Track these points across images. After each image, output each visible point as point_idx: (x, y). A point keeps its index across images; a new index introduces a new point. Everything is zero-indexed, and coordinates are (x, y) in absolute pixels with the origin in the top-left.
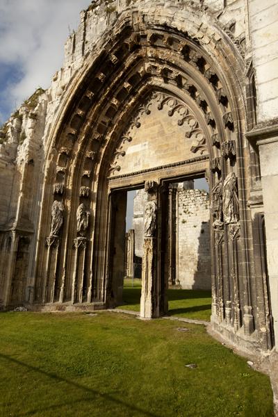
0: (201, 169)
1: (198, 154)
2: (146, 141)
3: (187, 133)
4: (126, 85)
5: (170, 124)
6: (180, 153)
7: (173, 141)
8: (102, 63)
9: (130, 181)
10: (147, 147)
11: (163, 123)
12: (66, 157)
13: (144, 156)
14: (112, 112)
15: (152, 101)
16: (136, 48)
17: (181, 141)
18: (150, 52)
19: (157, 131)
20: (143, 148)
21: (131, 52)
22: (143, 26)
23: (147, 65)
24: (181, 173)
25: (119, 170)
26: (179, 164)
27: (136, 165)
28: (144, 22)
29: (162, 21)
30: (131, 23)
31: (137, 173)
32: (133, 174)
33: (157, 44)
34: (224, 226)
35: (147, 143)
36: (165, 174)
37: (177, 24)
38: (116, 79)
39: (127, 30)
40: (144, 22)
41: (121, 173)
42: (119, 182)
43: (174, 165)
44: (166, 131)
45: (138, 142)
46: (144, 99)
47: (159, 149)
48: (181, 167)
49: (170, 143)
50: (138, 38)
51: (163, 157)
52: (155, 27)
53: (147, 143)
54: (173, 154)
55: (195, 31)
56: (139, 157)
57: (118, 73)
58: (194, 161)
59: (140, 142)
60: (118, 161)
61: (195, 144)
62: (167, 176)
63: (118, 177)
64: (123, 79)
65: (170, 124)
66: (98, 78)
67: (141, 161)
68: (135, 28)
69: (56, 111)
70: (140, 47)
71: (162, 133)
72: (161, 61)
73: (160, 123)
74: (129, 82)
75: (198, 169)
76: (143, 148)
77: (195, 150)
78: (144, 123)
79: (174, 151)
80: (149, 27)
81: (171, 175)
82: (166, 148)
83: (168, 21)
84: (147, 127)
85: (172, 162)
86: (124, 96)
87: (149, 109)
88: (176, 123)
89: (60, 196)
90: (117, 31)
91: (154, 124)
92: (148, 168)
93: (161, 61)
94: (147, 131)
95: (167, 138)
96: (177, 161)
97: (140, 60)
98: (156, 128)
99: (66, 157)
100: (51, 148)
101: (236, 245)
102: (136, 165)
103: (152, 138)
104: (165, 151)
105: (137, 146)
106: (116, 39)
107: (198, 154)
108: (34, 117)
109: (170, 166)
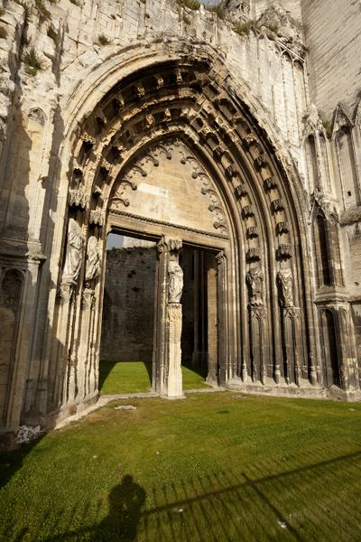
0: (220, 246)
1: (218, 231)
2: (165, 188)
3: (211, 206)
5: (193, 185)
7: (196, 205)
10: (167, 196)
12: (87, 147)
13: (164, 205)
14: (142, 129)
15: (172, 146)
16: (197, 88)
18: (206, 106)
19: (178, 184)
20: (162, 194)
21: (190, 87)
22: (221, 82)
23: (192, 113)
24: (202, 242)
25: (127, 206)
31: (157, 222)
33: (221, 107)
35: (167, 192)
36: (188, 236)
38: (166, 99)
39: (204, 66)
40: (225, 80)
41: (129, 210)
45: (153, 183)
46: (169, 139)
47: (181, 206)
48: (205, 237)
49: (193, 205)
50: (207, 83)
52: (234, 97)
54: (195, 220)
56: (157, 202)
57: (169, 94)
60: (124, 192)
61: (215, 220)
62: (190, 240)
63: (120, 213)
64: (168, 103)
66: (157, 81)
67: (159, 209)
68: (211, 73)
69: (95, 68)
70: (200, 91)
71: (185, 191)
72: (214, 125)
74: (171, 111)
77: (215, 226)
78: (163, 166)
79: (196, 216)
80: (228, 90)
81: (193, 241)
83: (251, 107)
84: (168, 173)
87: (187, 162)
88: (199, 189)
91: (175, 175)
92: (167, 221)
93: (214, 125)
94: (169, 178)
95: (190, 199)
96: (199, 229)
97: (191, 102)
98: (178, 181)
100: (75, 123)
102: (152, 210)
103: (173, 189)
105: (154, 187)
106: (191, 62)
107: (218, 231)
108: (51, 33)
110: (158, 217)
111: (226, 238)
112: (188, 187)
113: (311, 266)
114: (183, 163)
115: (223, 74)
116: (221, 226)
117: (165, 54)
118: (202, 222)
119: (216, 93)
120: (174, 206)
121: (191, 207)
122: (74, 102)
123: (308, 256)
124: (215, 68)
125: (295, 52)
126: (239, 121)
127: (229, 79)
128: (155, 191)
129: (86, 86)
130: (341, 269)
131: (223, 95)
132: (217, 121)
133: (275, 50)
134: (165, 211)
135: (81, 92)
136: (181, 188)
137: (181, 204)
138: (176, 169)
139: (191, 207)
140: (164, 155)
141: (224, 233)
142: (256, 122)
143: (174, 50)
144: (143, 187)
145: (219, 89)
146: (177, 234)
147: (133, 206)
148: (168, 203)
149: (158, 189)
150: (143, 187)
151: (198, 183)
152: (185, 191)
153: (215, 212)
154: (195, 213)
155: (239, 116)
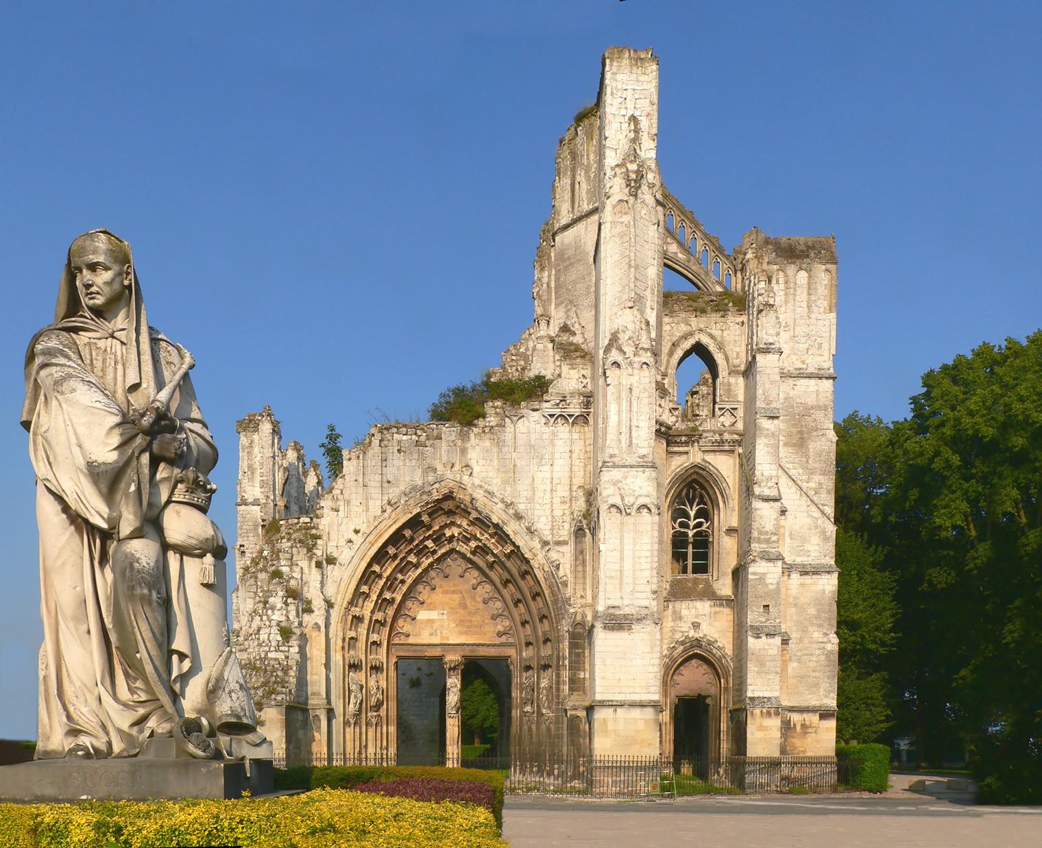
1: (504, 639)
4: (430, 544)
6: (485, 634)
8: (414, 523)
14: (403, 568)
18: (465, 523)
28: (471, 502)
29: (495, 520)
30: (455, 494)
32: (430, 645)
34: (540, 714)
37: (508, 530)
39: (449, 497)
43: (478, 645)
50: (458, 507)
54: (476, 633)
55: (527, 551)
58: (499, 645)
73: (461, 593)
75: (503, 654)
77: (500, 634)
80: (476, 510)
83: (500, 522)
86: (421, 551)
90: (436, 496)
99: (358, 619)
100: (343, 609)
101: (530, 729)
106: (434, 502)
107: (504, 639)
111: (510, 645)
113: (566, 675)
115: (468, 499)
116: (504, 634)
117: (405, 514)
119: (469, 513)
122: (339, 596)
123: (564, 665)
124: (459, 495)
125: (575, 409)
126: (495, 533)
127: (474, 502)
129: (346, 578)
130: (584, 678)
131: (474, 515)
132: (478, 536)
133: (544, 420)
135: (343, 585)
140: (428, 588)
141: (511, 640)
142: (508, 536)
143: (412, 505)
145: (469, 510)
151: (480, 593)
153: (499, 620)
155: (491, 531)
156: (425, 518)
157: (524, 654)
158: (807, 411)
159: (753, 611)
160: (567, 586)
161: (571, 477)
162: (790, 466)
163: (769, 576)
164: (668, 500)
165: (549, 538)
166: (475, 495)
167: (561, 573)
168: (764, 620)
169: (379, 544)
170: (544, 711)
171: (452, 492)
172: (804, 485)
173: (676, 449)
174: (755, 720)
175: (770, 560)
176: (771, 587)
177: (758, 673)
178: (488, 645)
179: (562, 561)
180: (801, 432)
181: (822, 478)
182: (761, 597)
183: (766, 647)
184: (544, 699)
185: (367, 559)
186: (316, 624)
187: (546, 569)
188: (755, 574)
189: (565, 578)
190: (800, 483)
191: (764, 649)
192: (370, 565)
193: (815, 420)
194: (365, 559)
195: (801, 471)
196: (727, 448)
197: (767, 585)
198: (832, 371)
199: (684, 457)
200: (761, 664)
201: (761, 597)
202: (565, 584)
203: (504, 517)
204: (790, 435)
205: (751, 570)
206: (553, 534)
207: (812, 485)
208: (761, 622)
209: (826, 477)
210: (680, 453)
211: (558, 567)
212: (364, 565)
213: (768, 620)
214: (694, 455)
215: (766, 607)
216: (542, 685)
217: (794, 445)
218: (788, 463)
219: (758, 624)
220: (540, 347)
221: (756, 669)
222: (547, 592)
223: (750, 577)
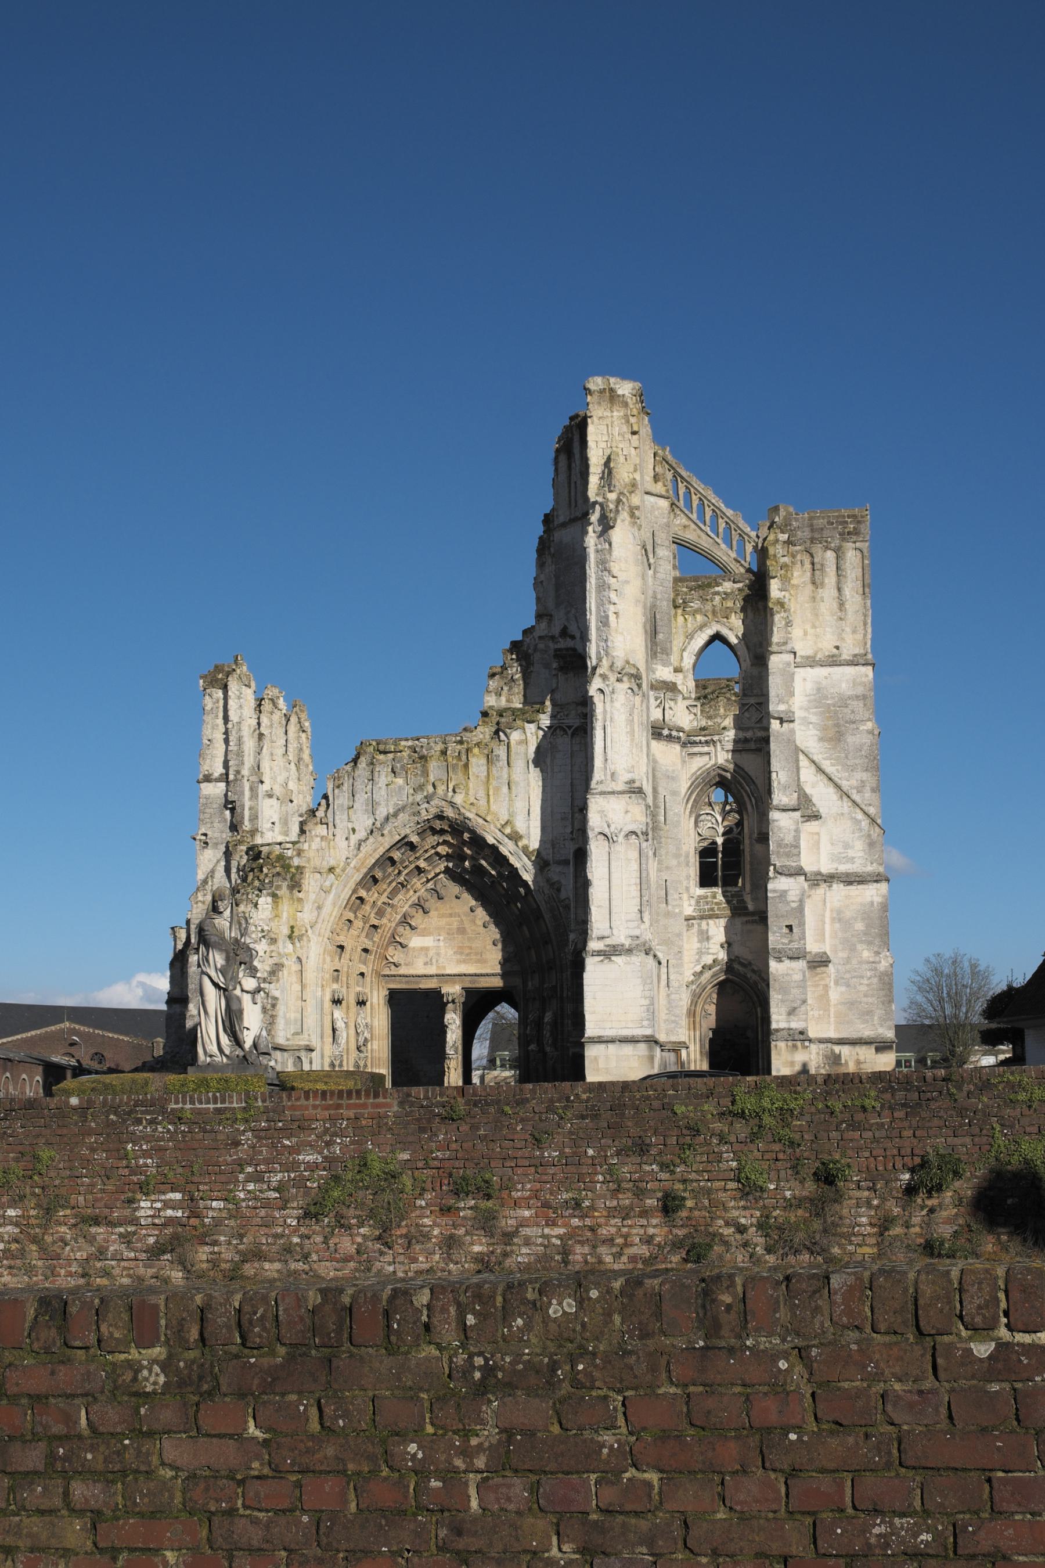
7: (477, 944)
9: (418, 983)
10: (442, 944)
11: (464, 918)
13: (438, 954)
17: (488, 947)
19: (455, 925)
20: (436, 944)
26: (487, 975)
27: (426, 964)
29: (491, 840)
35: (442, 938)
37: (504, 850)
41: (402, 971)
42: (400, 982)
44: (469, 931)
45: (425, 933)
47: (460, 951)
48: (487, 979)
49: (474, 946)
51: (464, 961)
53: (442, 938)
54: (478, 961)
56: (431, 953)
59: (429, 934)
62: (470, 986)
63: (394, 976)
65: (474, 922)
67: (434, 961)
76: (436, 944)
78: (436, 909)
79: (479, 957)
81: (474, 986)
82: (467, 951)
84: (442, 916)
85: (478, 972)
88: (480, 923)
89: (337, 1002)
90: (425, 816)
91: (451, 915)
94: (443, 922)
95: (469, 939)
96: (484, 971)
102: (426, 964)
104: (467, 955)
105: (427, 938)
109: (476, 975)
110: (432, 970)
112: (467, 925)
114: (457, 897)
118: (485, 961)
120: (450, 952)
121: (471, 948)
124: (450, 813)
128: (428, 941)
134: (441, 960)
136: (458, 929)
137: (460, 947)
138: (451, 908)
139: (471, 948)
144: (416, 942)
146: (455, 983)
147: (406, 965)
148: (443, 951)
149: (432, 938)
150: (416, 942)
152: (462, 931)
154: (476, 954)
156: (414, 839)
157: (530, 984)
158: (843, 701)
159: (774, 933)
160: (569, 909)
161: (572, 791)
162: (828, 762)
163: (790, 893)
164: (689, 805)
165: (550, 858)
166: (468, 814)
167: (563, 895)
168: (786, 941)
169: (365, 870)
170: (548, 1049)
171: (442, 812)
172: (845, 784)
173: (696, 750)
174: (779, 1054)
175: (790, 875)
176: (794, 905)
177: (782, 1001)
178: (493, 975)
179: (563, 882)
180: (837, 725)
181: (865, 776)
182: (782, 916)
183: (791, 972)
184: (548, 1034)
185: (352, 885)
186: (298, 958)
187: (546, 892)
188: (775, 891)
189: (567, 902)
190: (839, 782)
191: (787, 975)
192: (355, 891)
193: (853, 712)
194: (349, 886)
195: (839, 768)
196: (752, 746)
197: (788, 903)
198: (870, 656)
199: (707, 758)
200: (784, 990)
201: (782, 916)
202: (567, 907)
203: (499, 835)
204: (824, 728)
205: (770, 886)
206: (553, 853)
207: (854, 783)
208: (783, 944)
209: (869, 774)
210: (701, 754)
211: (559, 890)
212: (347, 893)
213: (791, 941)
214: (716, 756)
215: (790, 927)
216: (546, 1020)
217: (830, 740)
218: (824, 759)
219: (781, 946)
220: (541, 646)
221: (780, 997)
222: (547, 916)
223: (769, 895)
